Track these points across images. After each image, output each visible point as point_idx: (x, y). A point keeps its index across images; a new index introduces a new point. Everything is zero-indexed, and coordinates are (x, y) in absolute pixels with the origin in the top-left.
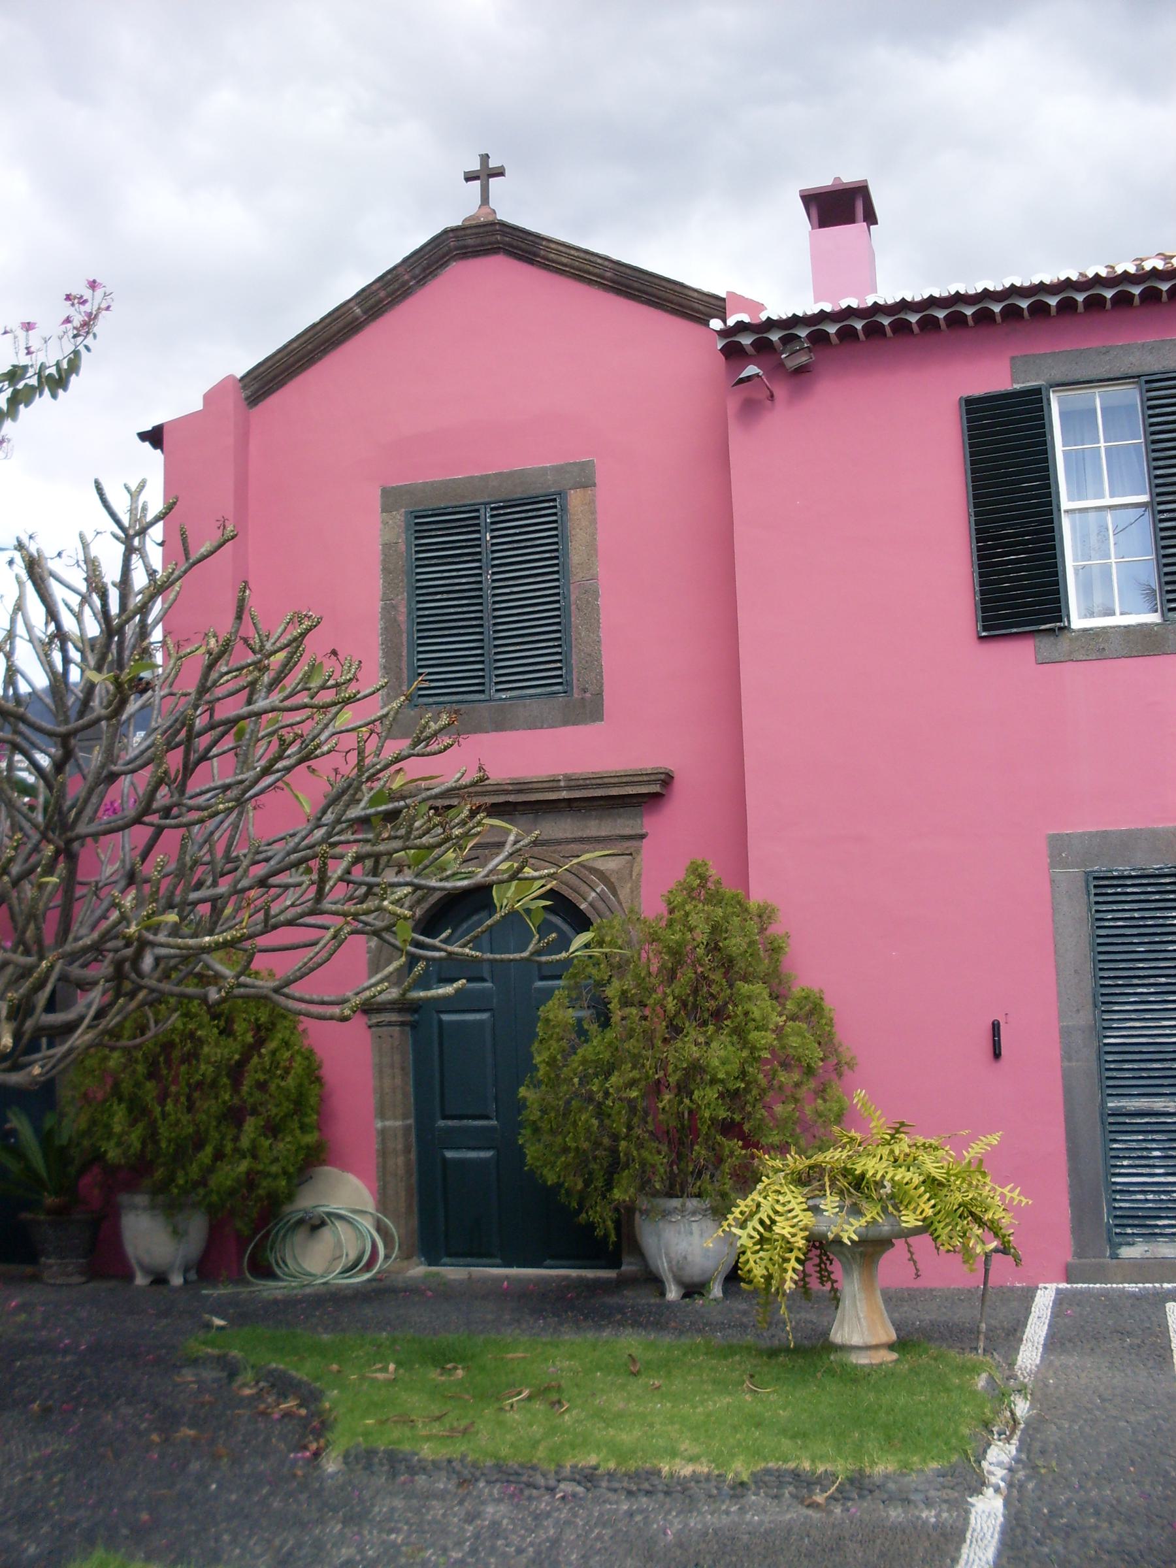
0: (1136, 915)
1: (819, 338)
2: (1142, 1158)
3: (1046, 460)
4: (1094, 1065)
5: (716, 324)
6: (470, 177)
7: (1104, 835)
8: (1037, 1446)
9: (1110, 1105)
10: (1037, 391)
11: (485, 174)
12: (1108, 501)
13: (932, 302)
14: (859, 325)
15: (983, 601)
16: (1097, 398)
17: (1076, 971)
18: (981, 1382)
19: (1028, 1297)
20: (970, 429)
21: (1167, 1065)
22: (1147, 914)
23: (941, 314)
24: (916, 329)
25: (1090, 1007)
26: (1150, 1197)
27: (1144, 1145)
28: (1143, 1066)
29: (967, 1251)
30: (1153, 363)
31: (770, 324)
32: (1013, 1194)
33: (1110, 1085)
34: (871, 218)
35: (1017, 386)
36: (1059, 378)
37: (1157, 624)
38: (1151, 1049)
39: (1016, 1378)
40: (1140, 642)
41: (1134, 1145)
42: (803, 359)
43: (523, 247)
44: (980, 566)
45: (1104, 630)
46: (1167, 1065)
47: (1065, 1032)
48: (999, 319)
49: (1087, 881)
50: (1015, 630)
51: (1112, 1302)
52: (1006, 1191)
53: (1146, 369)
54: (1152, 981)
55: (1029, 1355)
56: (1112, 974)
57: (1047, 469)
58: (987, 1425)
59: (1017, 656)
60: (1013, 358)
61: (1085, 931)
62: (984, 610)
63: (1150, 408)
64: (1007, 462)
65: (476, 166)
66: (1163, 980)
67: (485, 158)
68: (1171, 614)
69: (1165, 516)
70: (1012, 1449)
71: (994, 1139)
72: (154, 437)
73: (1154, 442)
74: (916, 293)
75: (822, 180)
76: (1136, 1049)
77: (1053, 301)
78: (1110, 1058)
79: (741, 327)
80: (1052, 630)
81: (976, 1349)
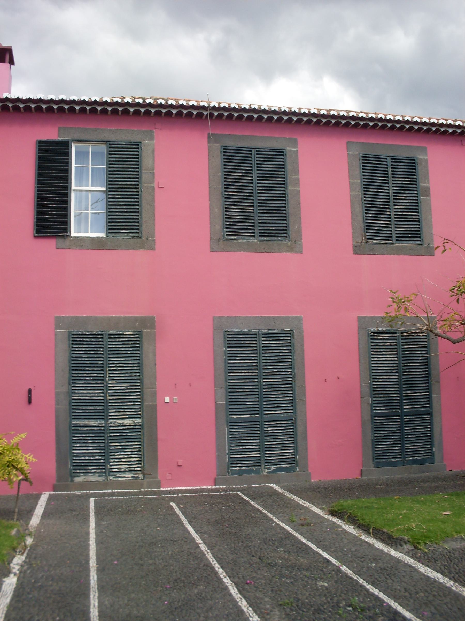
0: (87, 349)
2: (84, 443)
3: (68, 169)
4: (68, 407)
7: (77, 318)
8: (33, 556)
9: (73, 423)
10: (67, 142)
12: (90, 188)
13: (30, 100)
15: (37, 222)
16: (90, 148)
17: (63, 370)
18: (14, 532)
19: (38, 497)
20: (39, 153)
21: (95, 408)
22: (91, 349)
23: (33, 106)
24: (22, 110)
25: (67, 384)
26: (87, 458)
27: (85, 438)
28: (86, 408)
29: (10, 480)
30: (113, 138)
32: (30, 457)
33: (74, 415)
34: (12, 62)
35: (60, 139)
36: (76, 138)
37: (104, 238)
38: (90, 401)
39: (28, 529)
40: (96, 244)
41: (81, 438)
44: (38, 208)
45: (84, 238)
46: (95, 408)
47: (57, 394)
48: (56, 111)
49: (69, 335)
50: (49, 235)
51: (70, 498)
52: (27, 456)
54: (92, 375)
55: (35, 521)
56: (76, 372)
57: (68, 173)
58: (14, 549)
59: (48, 245)
60: (59, 127)
61: (67, 354)
62: (37, 226)
63: (110, 154)
64: (52, 168)
66: (96, 375)
68: (109, 235)
69: (111, 196)
70: (23, 558)
71: (23, 436)
73: (110, 168)
74: (24, 96)
76: (84, 401)
77: (78, 108)
78: (74, 404)
80: (63, 236)
81: (13, 519)
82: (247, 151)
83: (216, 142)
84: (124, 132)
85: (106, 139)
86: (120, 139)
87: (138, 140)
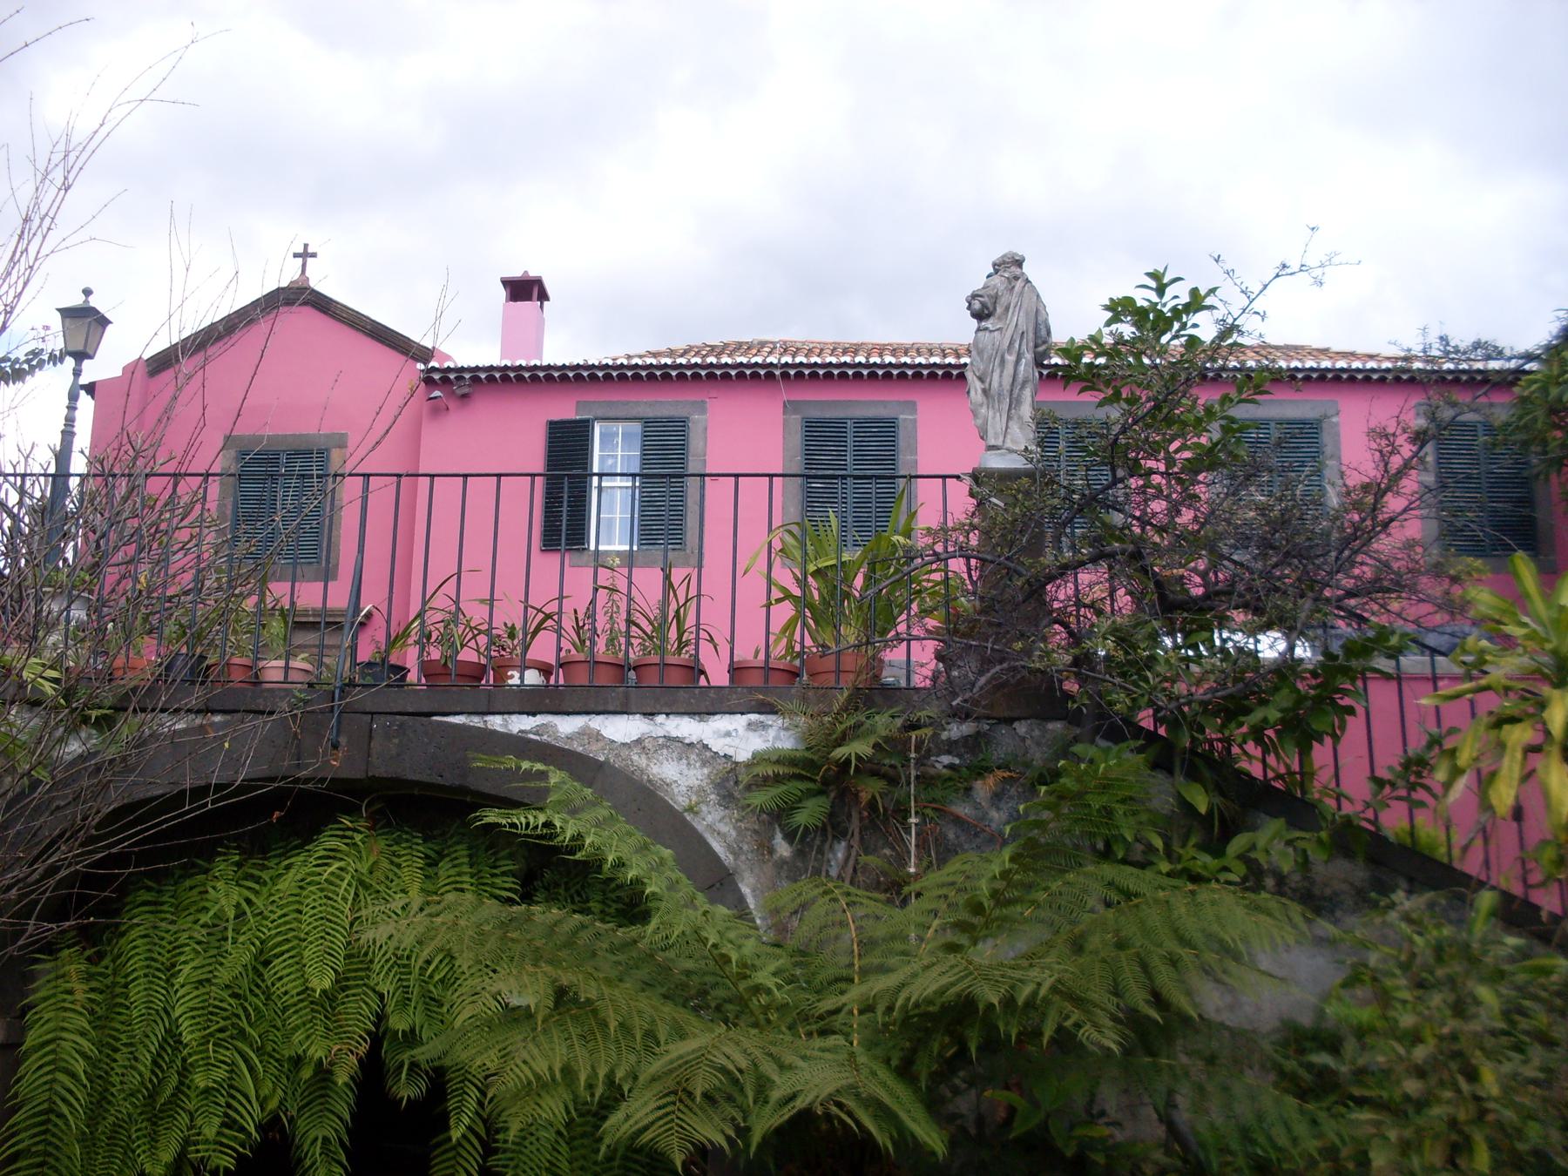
1: (476, 380)
5: (420, 366)
6: (296, 255)
10: (588, 421)
11: (305, 255)
14: (498, 375)
16: (620, 428)
30: (650, 413)
31: (449, 370)
34: (543, 296)
42: (466, 390)
43: (323, 305)
65: (301, 250)
67: (306, 246)
75: (516, 273)
79: (434, 369)
82: (839, 424)
83: (795, 411)
84: (665, 403)
86: (659, 414)
87: (685, 414)
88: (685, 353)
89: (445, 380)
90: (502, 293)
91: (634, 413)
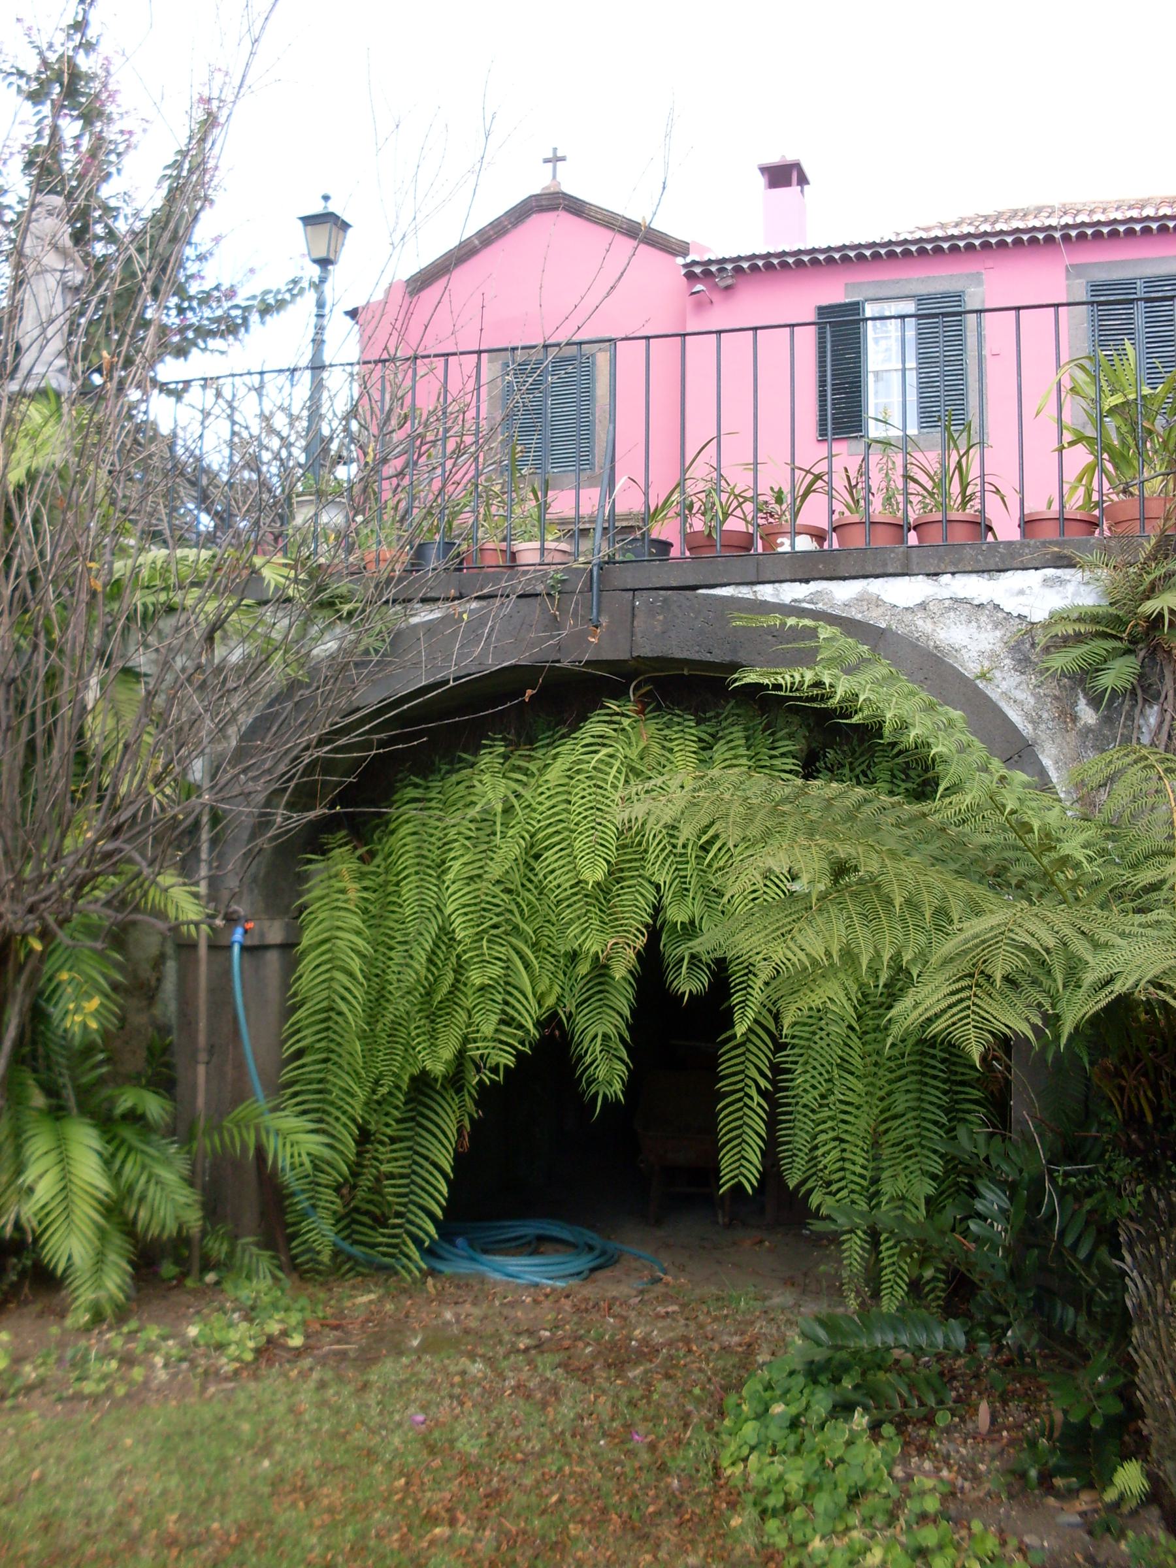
1: (738, 270)
5: (680, 261)
6: (547, 161)
10: (857, 303)
11: (555, 159)
31: (710, 262)
34: (803, 180)
42: (729, 282)
43: (576, 208)
53: (919, 292)
65: (550, 155)
72: (353, 314)
75: (773, 159)
79: (694, 263)
83: (1079, 276)
85: (913, 293)
88: (957, 225)
89: (707, 273)
90: (761, 181)
91: (907, 292)
